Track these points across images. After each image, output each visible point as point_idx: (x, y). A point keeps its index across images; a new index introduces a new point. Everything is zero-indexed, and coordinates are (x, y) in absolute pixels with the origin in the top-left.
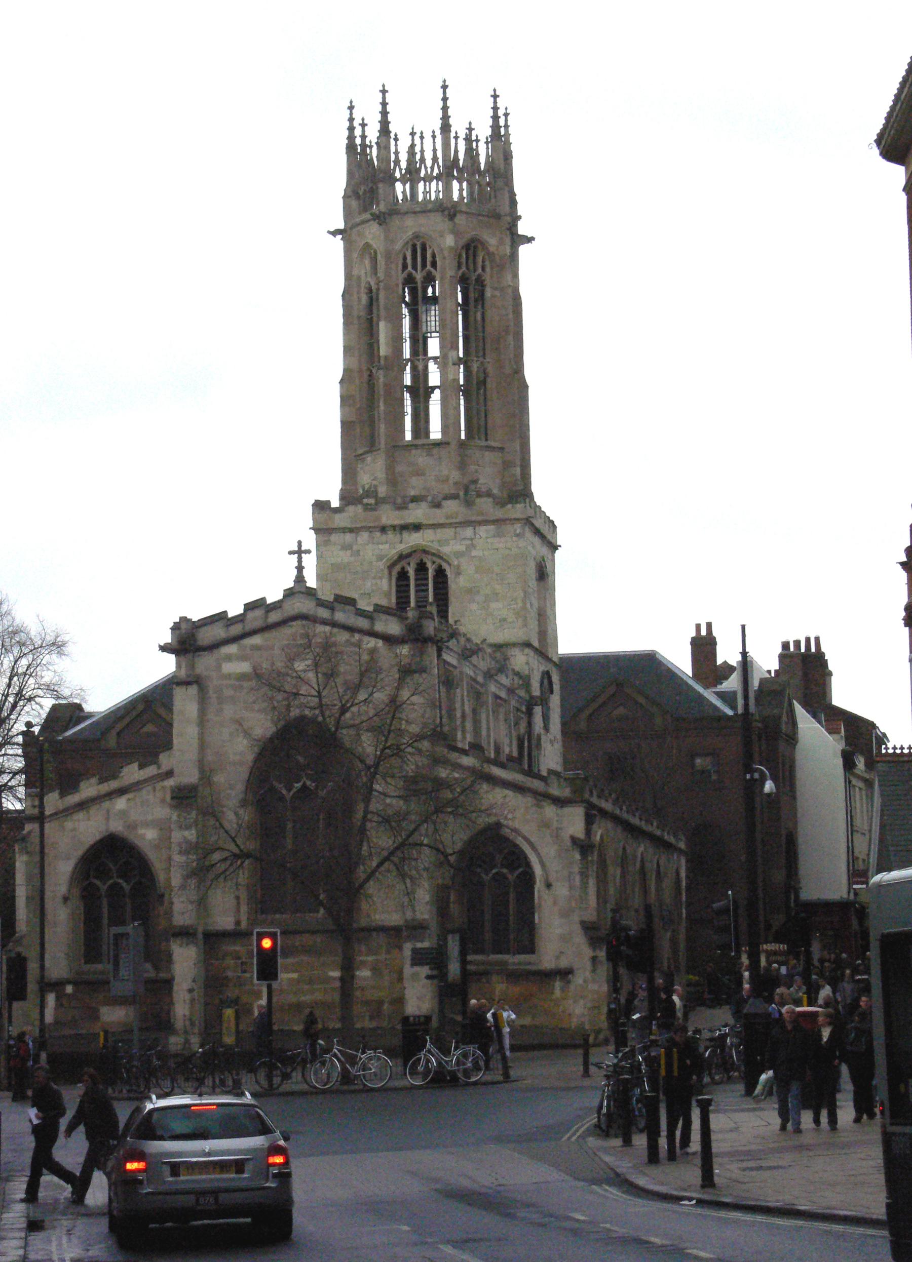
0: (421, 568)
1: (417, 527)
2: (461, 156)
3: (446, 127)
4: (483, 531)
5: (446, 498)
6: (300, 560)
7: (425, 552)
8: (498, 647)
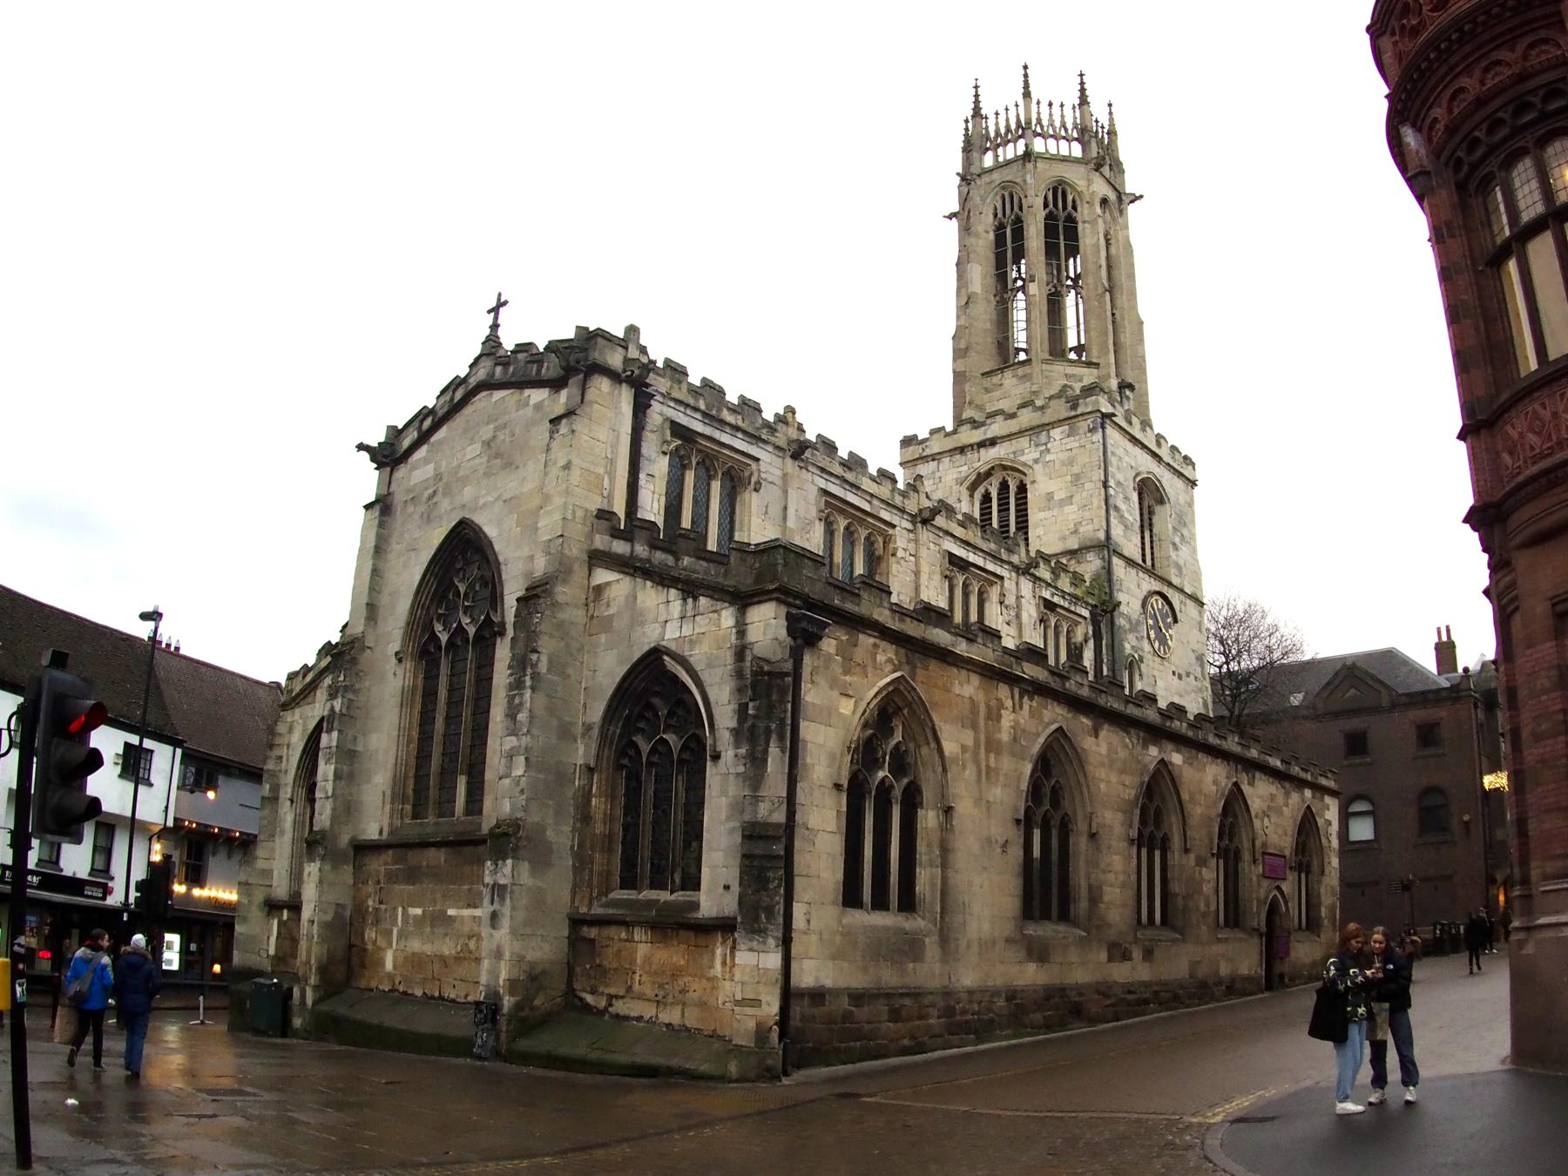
0: (1004, 487)
1: (992, 442)
4: (1056, 433)
5: (1023, 406)
6: (496, 318)
7: (1005, 468)
8: (1072, 553)
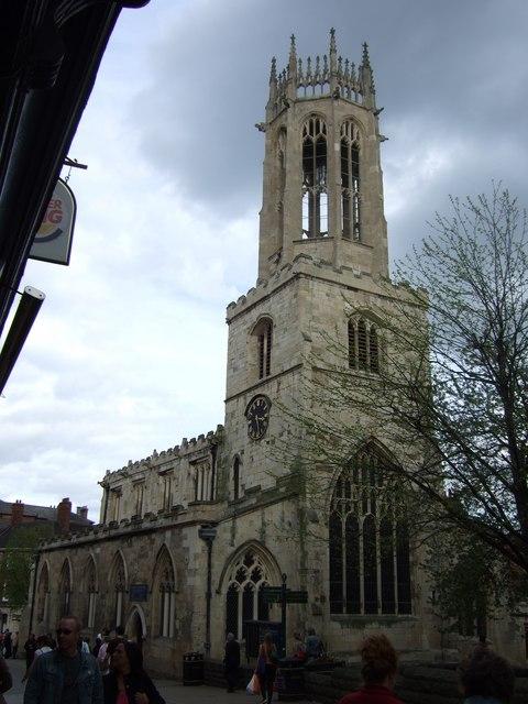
2: (343, 70)
3: (333, 50)
